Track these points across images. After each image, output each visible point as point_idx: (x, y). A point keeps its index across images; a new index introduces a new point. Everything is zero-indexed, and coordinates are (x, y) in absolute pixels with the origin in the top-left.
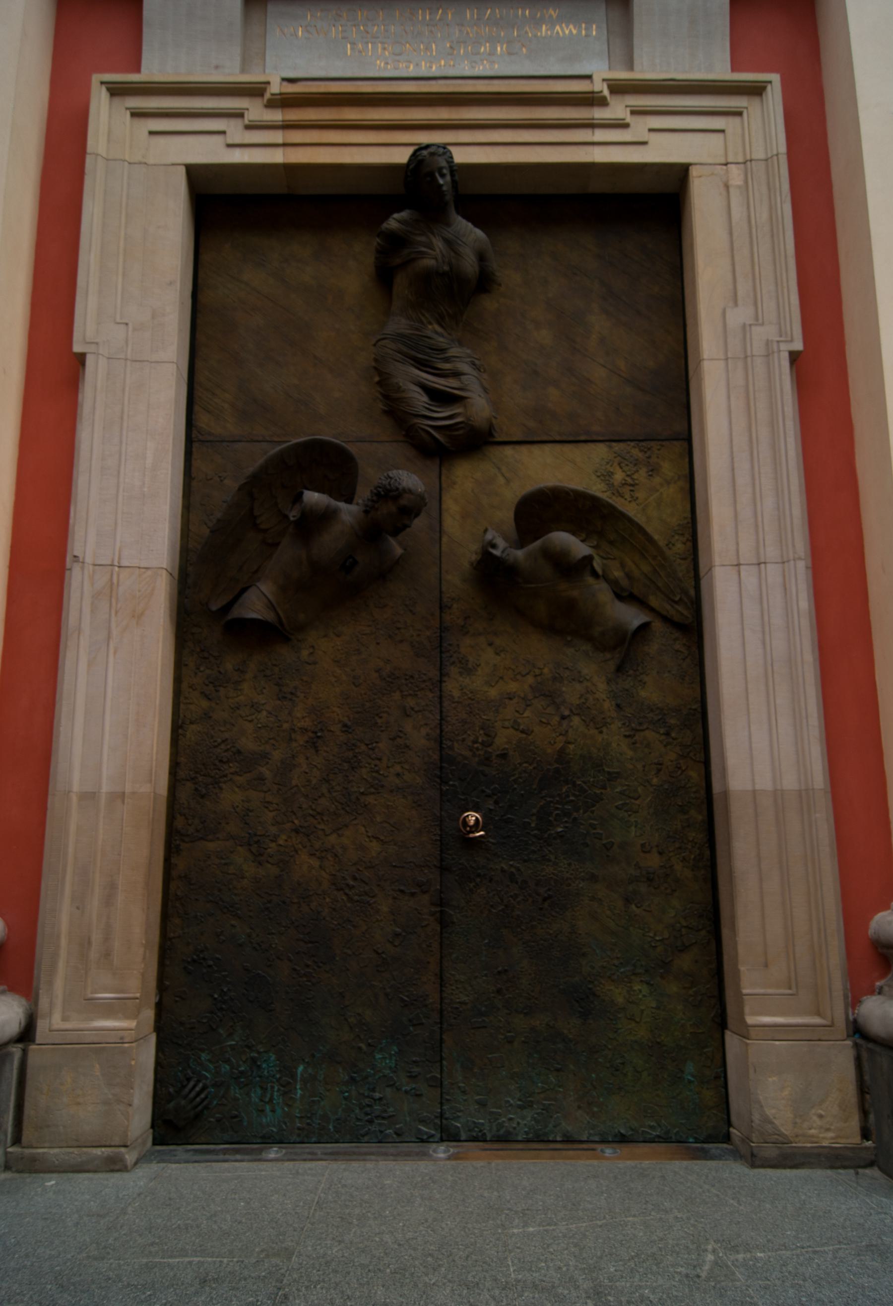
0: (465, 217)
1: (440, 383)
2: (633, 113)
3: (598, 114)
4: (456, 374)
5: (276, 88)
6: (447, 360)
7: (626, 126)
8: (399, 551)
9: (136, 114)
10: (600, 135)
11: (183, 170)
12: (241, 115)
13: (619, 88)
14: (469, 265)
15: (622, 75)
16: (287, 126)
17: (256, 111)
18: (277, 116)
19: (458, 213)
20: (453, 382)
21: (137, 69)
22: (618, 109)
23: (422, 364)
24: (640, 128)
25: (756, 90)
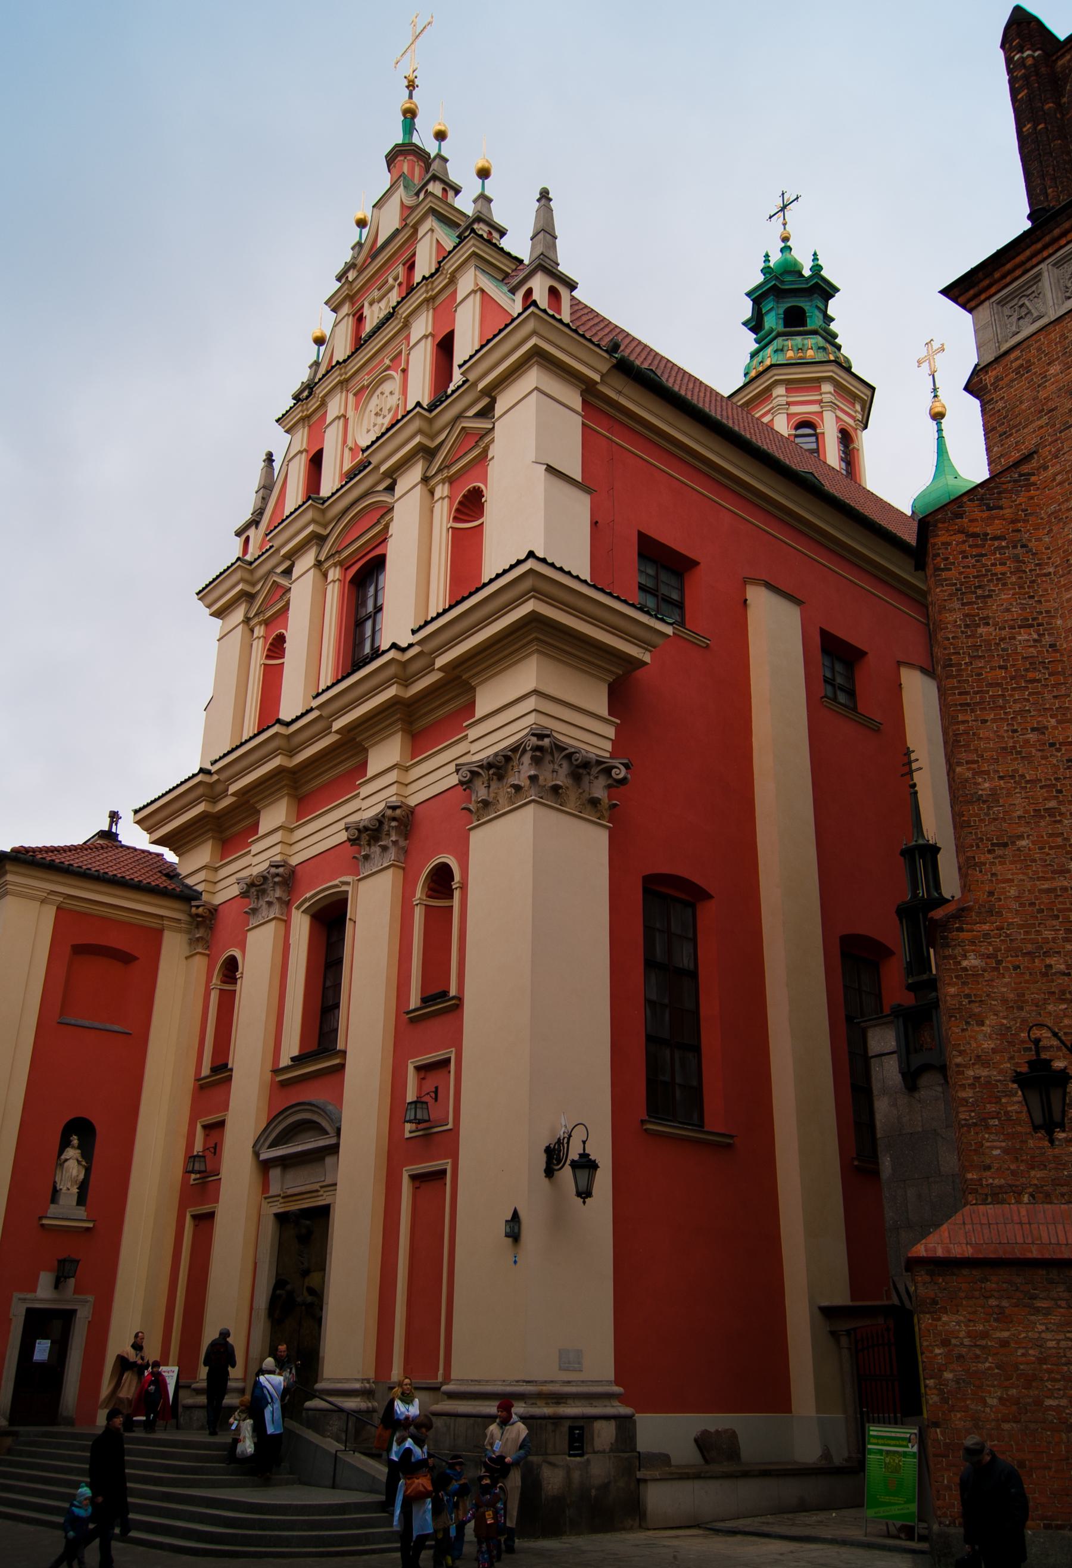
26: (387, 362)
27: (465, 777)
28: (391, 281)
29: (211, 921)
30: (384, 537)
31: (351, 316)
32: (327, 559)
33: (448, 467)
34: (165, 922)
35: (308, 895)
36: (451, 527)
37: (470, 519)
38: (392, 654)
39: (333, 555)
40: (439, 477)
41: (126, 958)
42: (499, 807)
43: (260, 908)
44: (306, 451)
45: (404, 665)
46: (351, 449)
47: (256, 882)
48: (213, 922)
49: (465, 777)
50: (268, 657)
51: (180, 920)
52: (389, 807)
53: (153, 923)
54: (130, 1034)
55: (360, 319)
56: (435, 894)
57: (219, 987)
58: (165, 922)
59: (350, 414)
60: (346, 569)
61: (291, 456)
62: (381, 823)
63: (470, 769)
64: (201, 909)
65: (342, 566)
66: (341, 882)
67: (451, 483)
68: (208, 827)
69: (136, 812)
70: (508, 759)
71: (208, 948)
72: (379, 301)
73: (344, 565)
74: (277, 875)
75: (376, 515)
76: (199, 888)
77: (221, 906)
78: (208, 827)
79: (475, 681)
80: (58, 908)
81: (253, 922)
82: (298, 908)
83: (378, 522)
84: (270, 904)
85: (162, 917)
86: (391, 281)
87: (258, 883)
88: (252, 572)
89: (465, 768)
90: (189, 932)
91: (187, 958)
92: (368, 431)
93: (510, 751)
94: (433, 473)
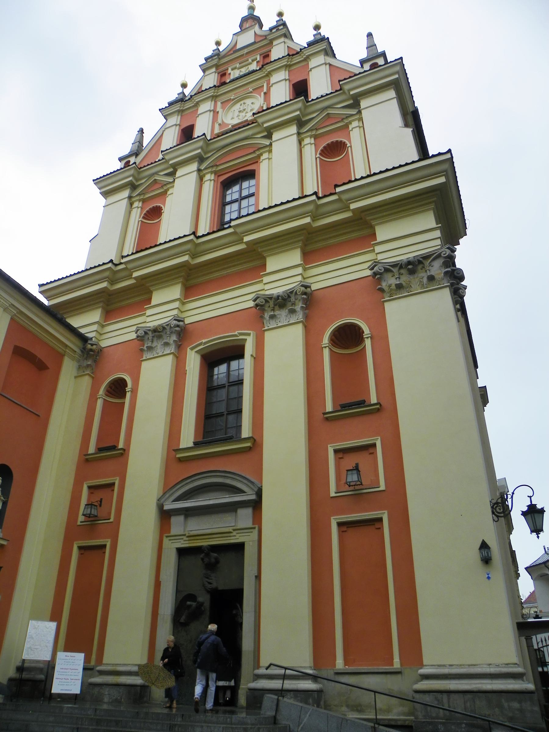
0: (213, 553)
1: (210, 581)
2: (237, 533)
3: (231, 534)
4: (212, 579)
5: (187, 535)
6: (211, 577)
7: (235, 536)
8: (203, 609)
9: (170, 540)
10: (232, 538)
11: (175, 549)
12: (182, 539)
13: (234, 530)
14: (213, 560)
15: (234, 528)
16: (188, 540)
17: (185, 538)
18: (187, 539)
19: (212, 552)
20: (211, 580)
21: (170, 533)
22: (234, 533)
23: (207, 578)
24: (238, 536)
25: (254, 528)
26: (251, 90)
27: (380, 270)
28: (250, 60)
29: (96, 357)
30: (257, 161)
31: (217, 74)
32: (205, 169)
33: (317, 129)
34: (67, 350)
35: (204, 341)
36: (319, 157)
37: (329, 158)
38: (314, 197)
39: (212, 166)
40: (309, 134)
41: (41, 366)
42: (412, 290)
43: (155, 347)
44: (180, 125)
45: (318, 207)
46: (220, 125)
47: (158, 329)
48: (98, 358)
49: (380, 270)
50: (144, 218)
51: (75, 352)
52: (302, 286)
53: (59, 348)
54: (39, 416)
55: (223, 75)
56: (334, 344)
57: (104, 398)
58: (67, 350)
59: (219, 109)
60: (219, 176)
61: (167, 126)
62: (289, 297)
63: (383, 266)
64: (94, 347)
65: (215, 174)
66: (239, 333)
67: (315, 139)
68: (102, 299)
69: (41, 286)
70: (420, 262)
71: (92, 373)
72: (239, 69)
73: (218, 174)
74: (178, 326)
75: (251, 150)
76: (89, 335)
77: (105, 349)
78: (102, 299)
79: (374, 222)
80: (12, 319)
81: (146, 355)
82: (192, 349)
83: (254, 152)
84: (167, 344)
85: (66, 346)
86: (250, 60)
87: (161, 330)
88: (139, 173)
89: (380, 265)
90: (78, 361)
91: (76, 377)
92: (233, 118)
93: (421, 258)
94: (305, 131)
